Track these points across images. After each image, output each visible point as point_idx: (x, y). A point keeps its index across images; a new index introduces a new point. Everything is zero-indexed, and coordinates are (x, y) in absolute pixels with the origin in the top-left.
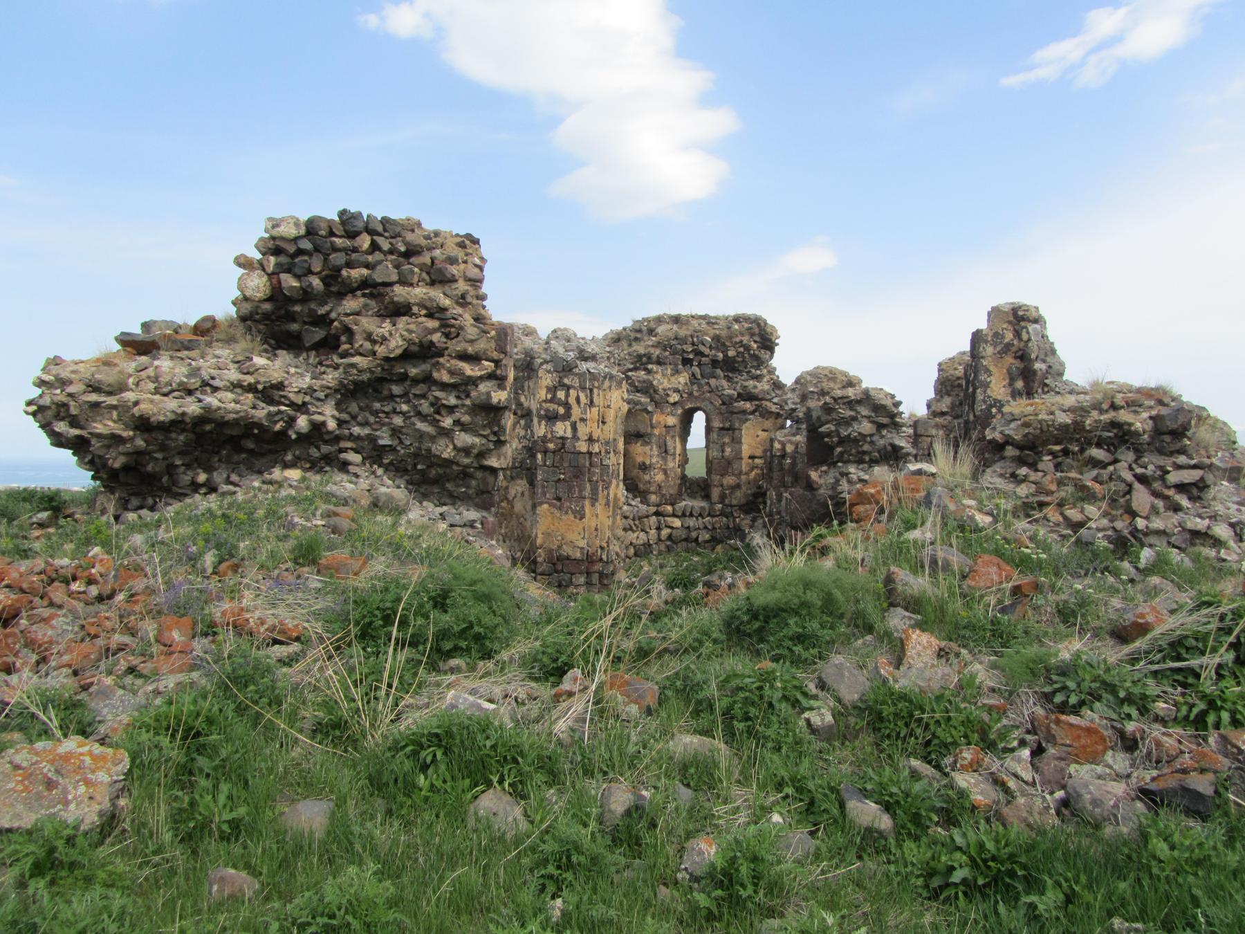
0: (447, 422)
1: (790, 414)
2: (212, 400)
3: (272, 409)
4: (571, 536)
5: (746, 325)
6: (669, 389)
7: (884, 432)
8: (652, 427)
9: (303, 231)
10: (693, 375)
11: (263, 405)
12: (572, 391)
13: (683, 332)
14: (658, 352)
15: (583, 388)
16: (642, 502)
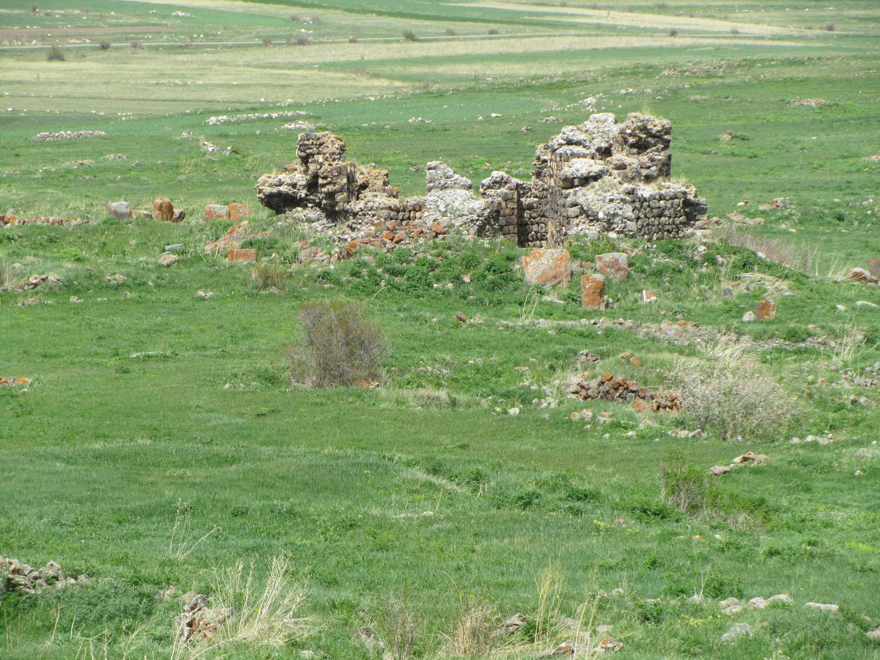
2: (281, 188)
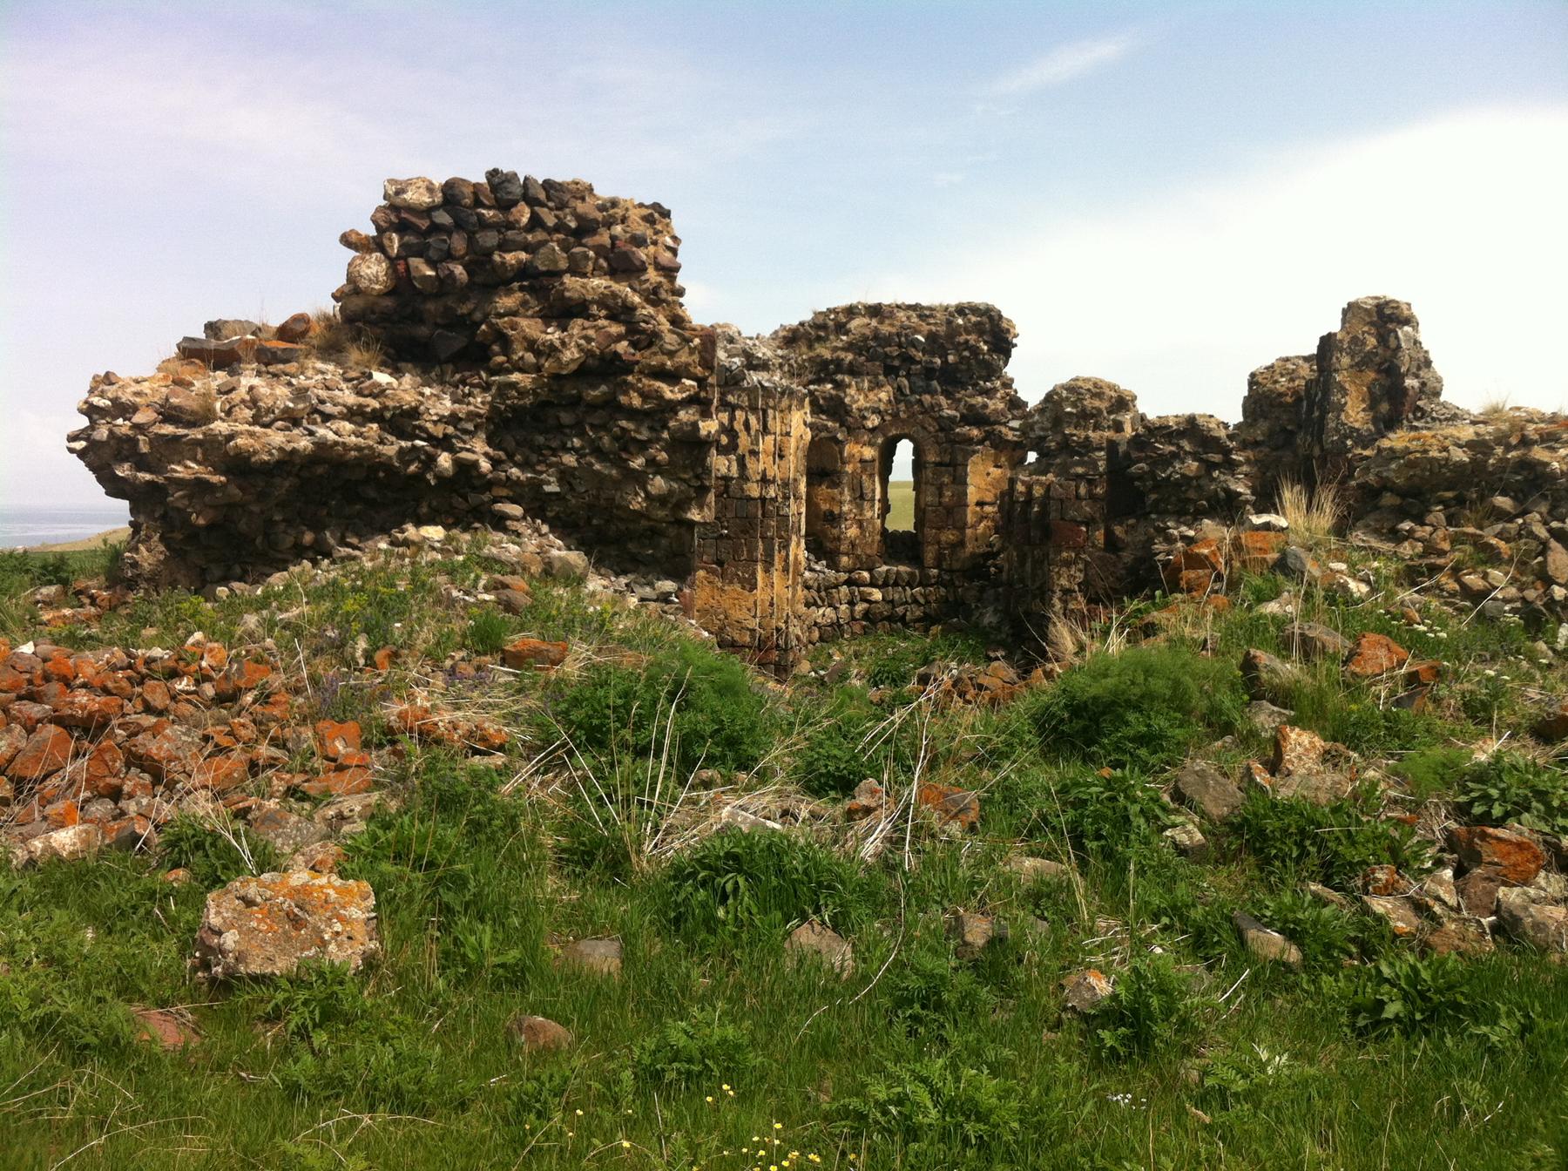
0: (638, 463)
1: (1037, 444)
2: (324, 432)
3: (403, 444)
4: (736, 614)
5: (974, 319)
6: (866, 409)
7: (1216, 474)
8: (844, 463)
9: (439, 198)
10: (900, 389)
11: (392, 438)
12: (738, 413)
13: (886, 329)
14: (850, 357)
15: (753, 409)
16: (828, 567)
